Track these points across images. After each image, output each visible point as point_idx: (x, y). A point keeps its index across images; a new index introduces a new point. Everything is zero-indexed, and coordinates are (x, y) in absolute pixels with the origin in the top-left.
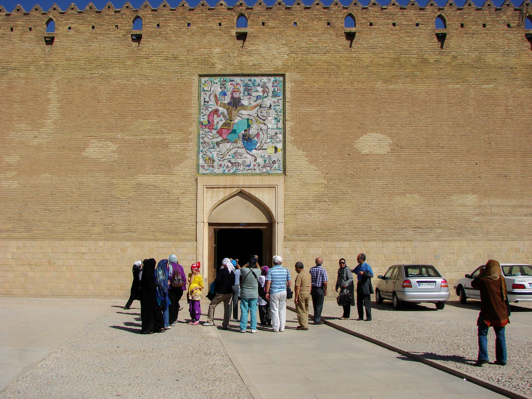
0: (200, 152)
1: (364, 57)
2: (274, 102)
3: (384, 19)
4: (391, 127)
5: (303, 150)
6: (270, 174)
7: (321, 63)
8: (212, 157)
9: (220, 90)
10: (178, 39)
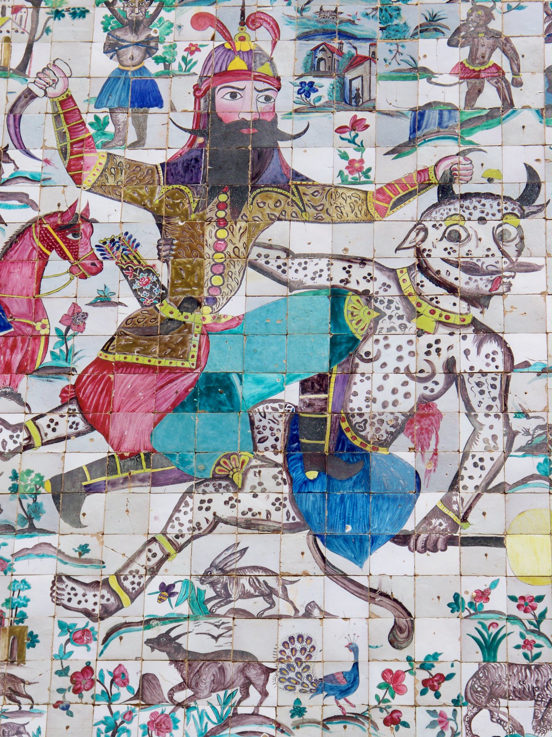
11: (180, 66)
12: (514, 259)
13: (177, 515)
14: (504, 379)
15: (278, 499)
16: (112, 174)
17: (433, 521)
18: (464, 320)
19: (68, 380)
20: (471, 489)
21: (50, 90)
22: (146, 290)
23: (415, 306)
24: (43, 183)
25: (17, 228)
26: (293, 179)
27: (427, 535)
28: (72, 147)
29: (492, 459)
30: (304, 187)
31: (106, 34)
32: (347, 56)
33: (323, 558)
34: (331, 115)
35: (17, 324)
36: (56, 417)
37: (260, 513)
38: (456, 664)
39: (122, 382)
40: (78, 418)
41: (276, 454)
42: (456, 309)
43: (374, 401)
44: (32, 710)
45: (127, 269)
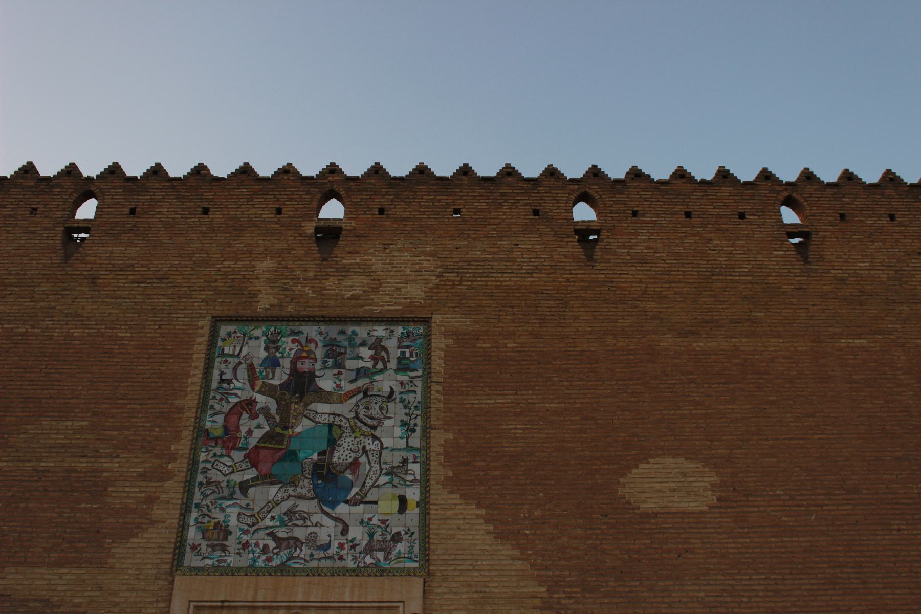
0: (194, 509)
1: (626, 282)
3: (664, 205)
4: (712, 441)
5: (479, 503)
6: (384, 570)
7: (520, 295)
8: (224, 521)
9: (263, 354)
10: (176, 239)
20: (368, 486)
25: (234, 404)
36: (242, 463)
40: (248, 464)
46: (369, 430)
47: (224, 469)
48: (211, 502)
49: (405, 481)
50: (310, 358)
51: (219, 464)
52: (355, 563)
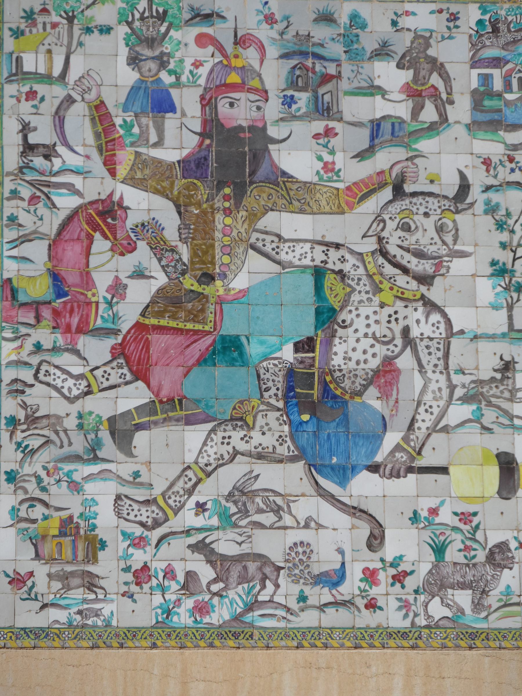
2: (487, 162)
6: (474, 635)
8: (81, 514)
11: (188, 78)
12: (451, 247)
13: (205, 448)
14: (446, 343)
15: (280, 437)
16: (139, 168)
17: (397, 454)
18: (415, 296)
19: (116, 339)
20: (424, 430)
21: (86, 96)
22: (171, 266)
23: (378, 283)
24: (86, 175)
26: (281, 177)
27: (392, 465)
28: (106, 146)
29: (438, 406)
30: (290, 184)
31: (127, 49)
32: (319, 74)
33: (317, 483)
34: (309, 124)
35: (74, 293)
36: (108, 369)
37: (268, 447)
38: (415, 563)
39: (157, 342)
40: (125, 371)
41: (278, 401)
42: (408, 287)
43: (350, 359)
44: (105, 598)
45: (156, 248)
46: (414, 284)
47: (67, 385)
48: (45, 468)
49: (511, 417)
50: (250, 90)
51: (52, 370)
52: (406, 616)
